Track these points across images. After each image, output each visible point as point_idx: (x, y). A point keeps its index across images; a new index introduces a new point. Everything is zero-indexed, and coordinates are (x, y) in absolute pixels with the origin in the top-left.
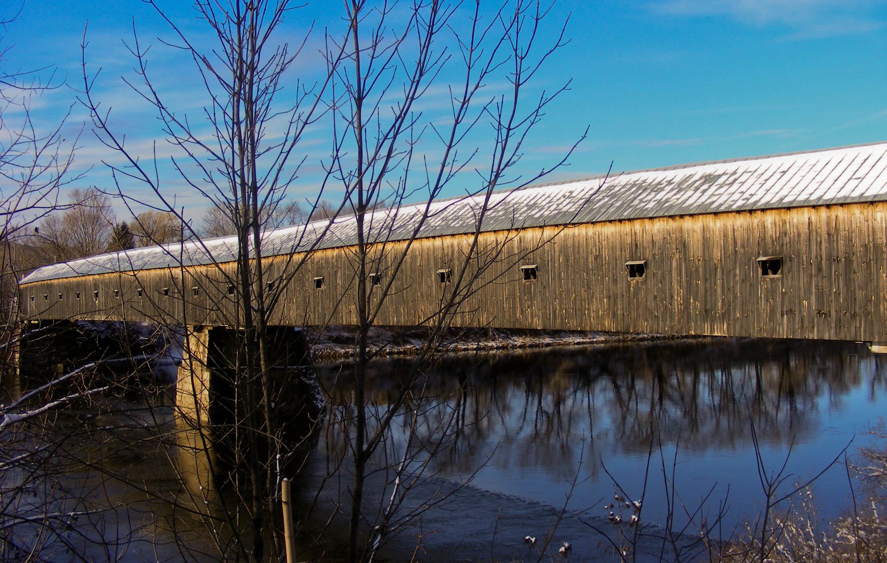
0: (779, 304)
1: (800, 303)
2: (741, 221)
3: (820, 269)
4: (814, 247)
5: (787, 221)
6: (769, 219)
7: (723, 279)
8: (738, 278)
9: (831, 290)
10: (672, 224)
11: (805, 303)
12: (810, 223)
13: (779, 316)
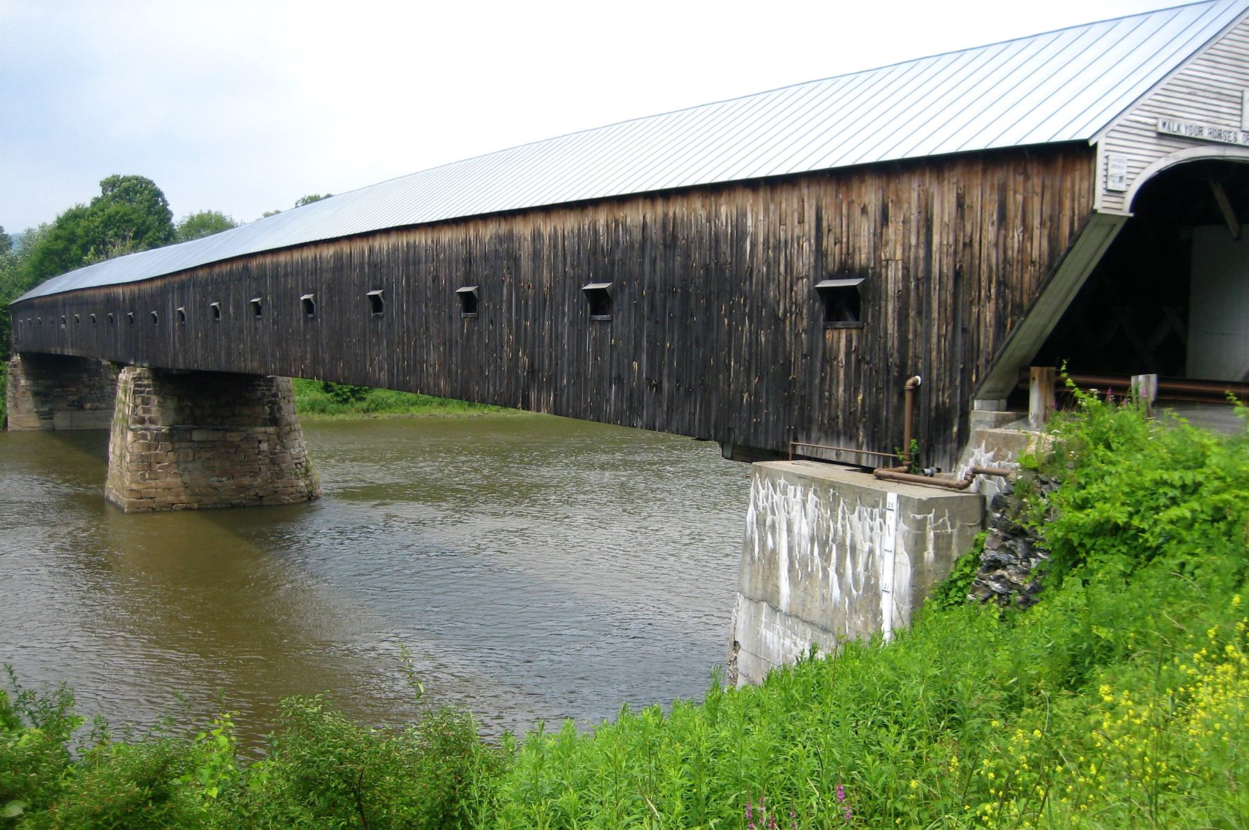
0: (607, 365)
1: (630, 366)
2: (570, 223)
3: (652, 307)
4: (647, 268)
5: (621, 219)
6: (602, 218)
7: (552, 320)
8: (566, 320)
9: (664, 345)
10: (503, 228)
11: (635, 365)
12: (644, 225)
13: (606, 386)
